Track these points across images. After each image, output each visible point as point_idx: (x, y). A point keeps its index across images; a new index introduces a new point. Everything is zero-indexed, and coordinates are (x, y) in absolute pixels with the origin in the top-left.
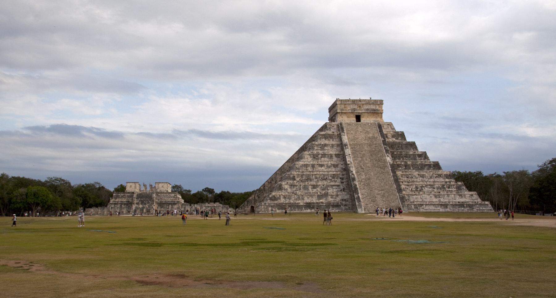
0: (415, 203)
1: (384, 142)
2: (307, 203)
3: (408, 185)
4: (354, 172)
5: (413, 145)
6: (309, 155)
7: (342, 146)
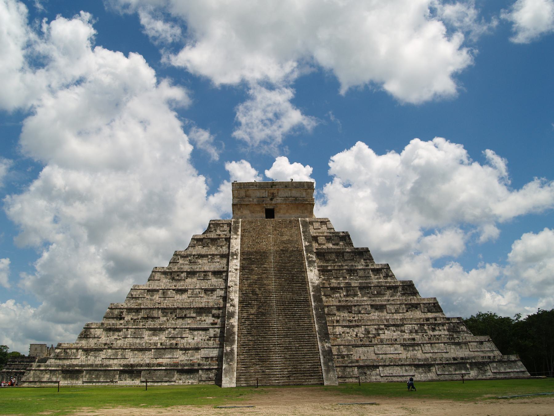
0: (361, 364)
2: (124, 366)
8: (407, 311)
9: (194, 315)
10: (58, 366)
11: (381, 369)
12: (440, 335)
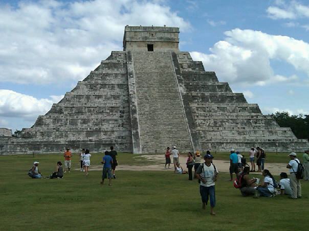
1: (178, 72)
2: (68, 142)
3: (204, 120)
5: (212, 76)
7: (127, 75)
8: (240, 111)
9: (108, 111)
10: (25, 142)
11: (225, 144)
12: (260, 126)
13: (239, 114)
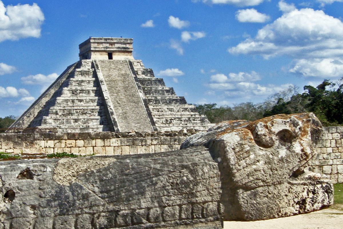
3: (159, 118)
4: (112, 107)
6: (69, 90)
7: (97, 83)
8: (182, 111)
9: (90, 112)
13: (183, 113)
